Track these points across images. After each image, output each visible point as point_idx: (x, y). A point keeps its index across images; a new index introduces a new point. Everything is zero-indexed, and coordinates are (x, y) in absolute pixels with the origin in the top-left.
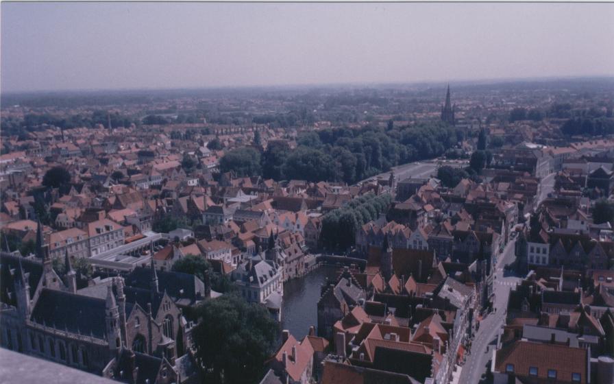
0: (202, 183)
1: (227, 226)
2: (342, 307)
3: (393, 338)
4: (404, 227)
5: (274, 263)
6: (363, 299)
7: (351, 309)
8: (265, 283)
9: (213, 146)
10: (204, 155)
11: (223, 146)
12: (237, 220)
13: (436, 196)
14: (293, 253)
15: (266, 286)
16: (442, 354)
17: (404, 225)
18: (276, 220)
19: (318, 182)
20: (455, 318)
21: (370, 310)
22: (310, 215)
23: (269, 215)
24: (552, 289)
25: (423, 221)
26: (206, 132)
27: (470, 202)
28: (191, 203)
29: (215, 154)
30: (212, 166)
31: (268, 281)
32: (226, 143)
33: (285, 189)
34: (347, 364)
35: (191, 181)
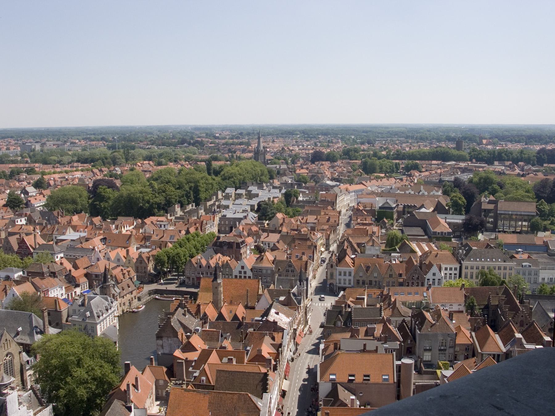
0: (30, 221)
1: (59, 264)
2: (180, 337)
3: (230, 360)
4: (229, 259)
5: (109, 298)
6: (198, 328)
7: (188, 337)
8: (101, 318)
9: (39, 185)
10: (30, 194)
11: (49, 185)
12: (69, 257)
13: (254, 228)
14: (126, 287)
15: (103, 320)
16: (274, 371)
17: (230, 257)
18: (106, 257)
19: (145, 218)
20: (282, 339)
21: (206, 336)
22: (140, 251)
23: (100, 251)
24: (360, 306)
25: (246, 252)
26: (31, 171)
27: (286, 234)
28: (22, 242)
29: (41, 194)
30: (39, 205)
31: (104, 316)
32: (52, 183)
33: (114, 226)
34: (191, 388)
35: (19, 220)
